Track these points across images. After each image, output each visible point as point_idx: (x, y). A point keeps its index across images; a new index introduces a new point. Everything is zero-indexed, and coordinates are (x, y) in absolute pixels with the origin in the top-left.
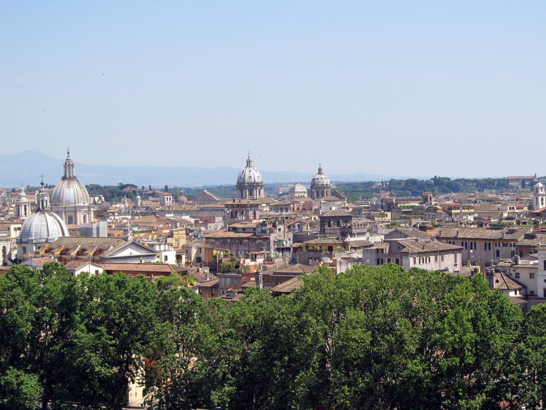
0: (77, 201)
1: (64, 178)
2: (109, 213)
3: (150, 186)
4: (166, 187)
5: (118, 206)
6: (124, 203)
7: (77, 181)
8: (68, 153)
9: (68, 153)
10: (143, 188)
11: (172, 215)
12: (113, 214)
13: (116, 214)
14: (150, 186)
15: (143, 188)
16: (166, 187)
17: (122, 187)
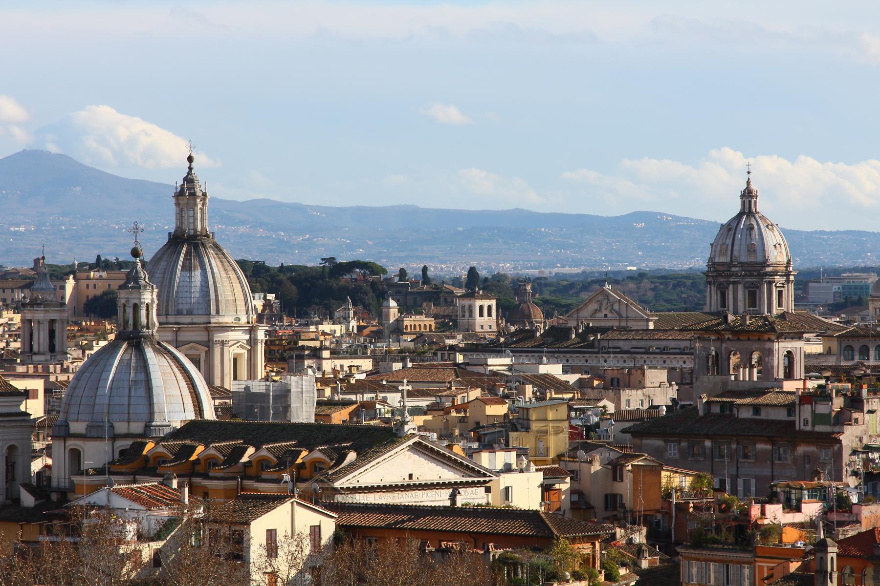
0: (213, 312)
1: (176, 240)
2: (303, 348)
3: (425, 269)
4: (472, 272)
5: (326, 327)
6: (346, 319)
7: (216, 247)
8: (190, 159)
9: (190, 159)
10: (402, 273)
11: (507, 361)
12: (316, 353)
13: (326, 354)
14: (425, 269)
15: (402, 273)
16: (472, 272)
17: (337, 269)
